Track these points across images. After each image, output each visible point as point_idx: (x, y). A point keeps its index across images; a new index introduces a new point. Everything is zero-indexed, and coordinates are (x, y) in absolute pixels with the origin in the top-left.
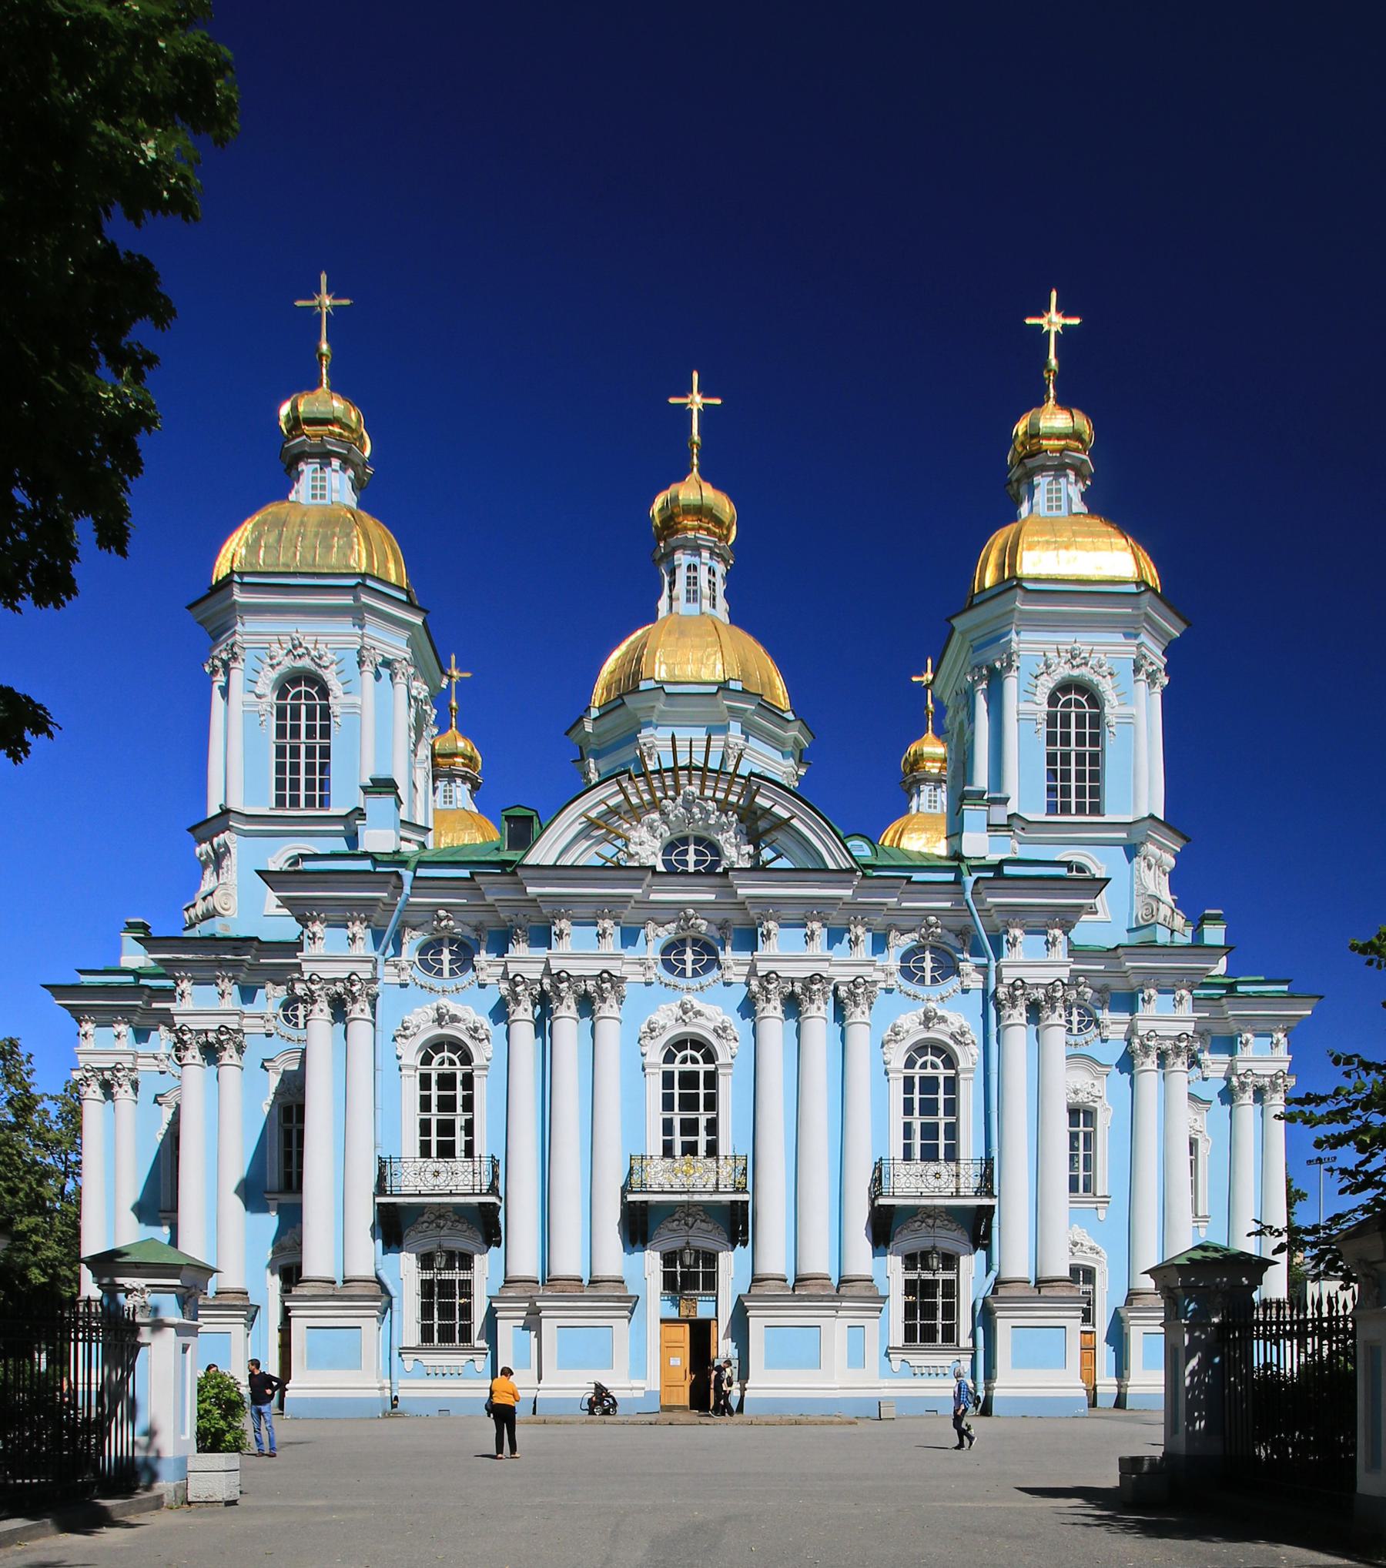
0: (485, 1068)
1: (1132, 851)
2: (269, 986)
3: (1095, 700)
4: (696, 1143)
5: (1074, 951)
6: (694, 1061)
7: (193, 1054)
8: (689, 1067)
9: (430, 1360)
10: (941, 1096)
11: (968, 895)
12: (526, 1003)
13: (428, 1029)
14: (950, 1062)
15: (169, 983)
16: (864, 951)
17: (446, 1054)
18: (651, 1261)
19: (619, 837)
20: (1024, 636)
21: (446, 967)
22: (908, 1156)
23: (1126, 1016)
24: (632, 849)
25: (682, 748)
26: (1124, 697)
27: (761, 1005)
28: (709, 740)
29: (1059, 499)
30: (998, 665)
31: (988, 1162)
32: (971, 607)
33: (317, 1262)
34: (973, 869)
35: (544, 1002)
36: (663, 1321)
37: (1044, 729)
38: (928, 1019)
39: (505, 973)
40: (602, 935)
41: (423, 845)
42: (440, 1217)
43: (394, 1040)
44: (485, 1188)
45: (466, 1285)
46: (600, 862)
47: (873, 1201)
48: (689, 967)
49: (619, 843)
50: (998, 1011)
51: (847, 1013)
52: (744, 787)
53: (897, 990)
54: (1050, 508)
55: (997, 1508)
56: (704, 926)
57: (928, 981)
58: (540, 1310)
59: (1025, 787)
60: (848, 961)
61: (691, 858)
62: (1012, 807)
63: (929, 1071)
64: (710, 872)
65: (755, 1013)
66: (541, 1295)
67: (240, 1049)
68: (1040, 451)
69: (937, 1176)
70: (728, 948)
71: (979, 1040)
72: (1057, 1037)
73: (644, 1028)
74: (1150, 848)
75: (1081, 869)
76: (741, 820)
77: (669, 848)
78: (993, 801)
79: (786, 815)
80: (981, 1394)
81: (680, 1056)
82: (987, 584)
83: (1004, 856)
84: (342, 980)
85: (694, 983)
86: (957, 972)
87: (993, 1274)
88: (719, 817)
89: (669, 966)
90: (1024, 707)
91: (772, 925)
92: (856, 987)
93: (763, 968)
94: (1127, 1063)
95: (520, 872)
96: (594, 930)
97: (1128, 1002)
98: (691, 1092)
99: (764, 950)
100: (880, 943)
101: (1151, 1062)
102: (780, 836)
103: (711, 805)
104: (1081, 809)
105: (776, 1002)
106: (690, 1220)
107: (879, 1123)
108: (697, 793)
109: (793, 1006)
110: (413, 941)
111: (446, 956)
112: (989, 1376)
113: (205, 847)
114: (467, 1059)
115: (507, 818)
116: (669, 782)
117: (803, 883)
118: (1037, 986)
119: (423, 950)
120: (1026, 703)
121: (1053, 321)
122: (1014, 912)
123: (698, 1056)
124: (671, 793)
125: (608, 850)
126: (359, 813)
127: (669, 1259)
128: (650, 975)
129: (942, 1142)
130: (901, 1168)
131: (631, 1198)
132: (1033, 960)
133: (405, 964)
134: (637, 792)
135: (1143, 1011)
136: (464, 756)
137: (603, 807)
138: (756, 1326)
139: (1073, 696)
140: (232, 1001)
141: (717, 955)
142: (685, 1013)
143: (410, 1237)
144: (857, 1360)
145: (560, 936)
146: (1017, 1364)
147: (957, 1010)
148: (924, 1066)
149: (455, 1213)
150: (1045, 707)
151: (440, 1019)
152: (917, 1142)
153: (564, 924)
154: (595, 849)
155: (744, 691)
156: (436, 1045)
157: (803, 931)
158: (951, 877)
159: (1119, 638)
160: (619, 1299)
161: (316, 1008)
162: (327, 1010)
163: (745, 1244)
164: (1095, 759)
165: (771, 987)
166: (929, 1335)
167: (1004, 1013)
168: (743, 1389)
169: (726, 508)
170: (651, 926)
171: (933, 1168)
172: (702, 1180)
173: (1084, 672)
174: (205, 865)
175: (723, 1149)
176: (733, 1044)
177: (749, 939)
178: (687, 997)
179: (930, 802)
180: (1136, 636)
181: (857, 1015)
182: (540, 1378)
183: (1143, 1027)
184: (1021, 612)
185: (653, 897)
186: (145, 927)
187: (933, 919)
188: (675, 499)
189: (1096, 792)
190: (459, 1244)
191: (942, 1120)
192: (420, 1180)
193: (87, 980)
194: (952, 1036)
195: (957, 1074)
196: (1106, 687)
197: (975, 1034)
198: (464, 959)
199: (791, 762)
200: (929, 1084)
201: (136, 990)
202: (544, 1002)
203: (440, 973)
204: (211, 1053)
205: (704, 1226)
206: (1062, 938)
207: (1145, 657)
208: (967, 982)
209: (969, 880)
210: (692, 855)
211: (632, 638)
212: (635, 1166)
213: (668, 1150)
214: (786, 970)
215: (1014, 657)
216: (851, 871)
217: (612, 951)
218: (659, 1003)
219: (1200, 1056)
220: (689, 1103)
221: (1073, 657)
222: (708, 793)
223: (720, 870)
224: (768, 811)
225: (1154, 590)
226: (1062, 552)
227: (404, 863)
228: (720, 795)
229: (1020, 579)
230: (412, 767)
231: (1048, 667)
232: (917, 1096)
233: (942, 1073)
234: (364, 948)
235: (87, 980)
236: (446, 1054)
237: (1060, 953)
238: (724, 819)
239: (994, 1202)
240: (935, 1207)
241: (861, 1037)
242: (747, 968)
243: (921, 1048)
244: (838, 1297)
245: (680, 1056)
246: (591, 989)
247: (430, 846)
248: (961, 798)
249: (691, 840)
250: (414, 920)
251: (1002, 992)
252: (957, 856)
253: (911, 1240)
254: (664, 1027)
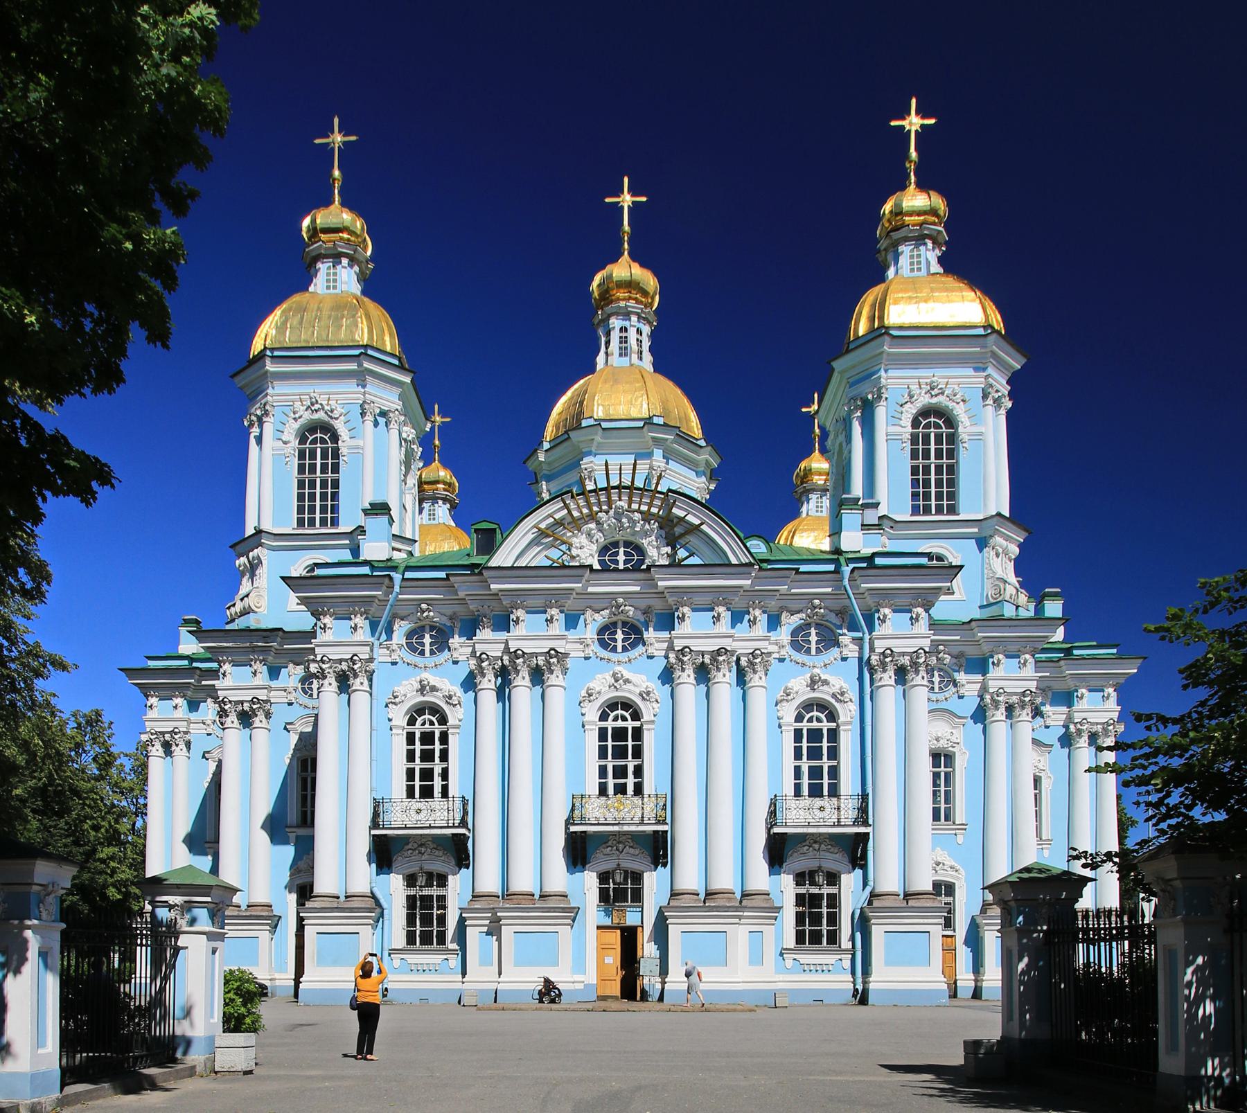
0: (458, 727)
1: (982, 543)
2: (291, 666)
3: (951, 422)
4: (625, 784)
5: (934, 625)
6: (624, 719)
7: (232, 720)
8: (620, 723)
9: (413, 959)
10: (825, 744)
11: (846, 582)
12: (490, 675)
13: (413, 697)
14: (832, 717)
15: (215, 665)
16: (761, 629)
17: (427, 717)
18: (590, 880)
19: (564, 543)
20: (891, 373)
21: (427, 648)
22: (798, 793)
23: (979, 677)
24: (574, 552)
25: (614, 471)
26: (975, 418)
27: (677, 673)
28: (635, 464)
29: (919, 263)
30: (870, 397)
31: (864, 797)
32: (848, 351)
33: (326, 881)
34: (849, 560)
35: (505, 675)
36: (599, 928)
37: (908, 446)
38: (813, 683)
39: (474, 652)
40: (549, 621)
41: (410, 554)
42: (421, 845)
43: (387, 706)
44: (457, 822)
45: (442, 899)
46: (549, 563)
47: (769, 830)
48: (620, 645)
49: (564, 547)
50: (871, 675)
51: (747, 679)
52: (663, 501)
53: (788, 660)
54: (912, 270)
55: (860, 1081)
56: (631, 611)
57: (813, 651)
58: (500, 919)
59: (893, 495)
60: (747, 638)
61: (621, 558)
62: (882, 510)
63: (815, 724)
64: (636, 569)
65: (672, 680)
66: (501, 907)
67: (268, 715)
68: (904, 226)
69: (822, 809)
70: (651, 629)
71: (856, 698)
72: (920, 695)
73: (584, 693)
74: (998, 540)
75: (940, 558)
76: (661, 527)
77: (603, 550)
78: (866, 506)
79: (697, 522)
80: (860, 987)
81: (612, 715)
82: (861, 333)
83: (875, 550)
84: (346, 660)
85: (624, 657)
86: (837, 644)
87: (868, 889)
88: (643, 526)
89: (603, 644)
90: (892, 429)
91: (686, 610)
92: (755, 658)
93: (678, 644)
94: (980, 715)
95: (485, 573)
96: (544, 616)
97: (980, 665)
98: (621, 743)
99: (679, 629)
100: (774, 622)
101: (1000, 714)
102: (692, 540)
103: (637, 516)
104: (939, 510)
105: (690, 671)
106: (621, 846)
107: (775, 766)
108: (626, 507)
109: (703, 674)
110: (401, 629)
111: (427, 640)
112: (866, 972)
113: (243, 560)
114: (443, 720)
115: (476, 530)
116: (603, 499)
117: (712, 576)
118: (904, 654)
119: (409, 635)
120: (893, 427)
121: (914, 122)
122: (885, 594)
123: (627, 715)
124: (605, 507)
125: (555, 554)
126: (361, 530)
127: (604, 877)
128: (589, 651)
129: (826, 781)
130: (792, 803)
131: (573, 829)
132: (899, 633)
133: (395, 647)
134: (578, 508)
135: (993, 672)
136: (444, 483)
137: (551, 520)
138: (674, 932)
139: (932, 420)
140: (262, 678)
141: (642, 634)
142: (616, 681)
143: (398, 861)
144: (756, 958)
145: (517, 622)
146: (888, 963)
147: (837, 674)
148: (810, 720)
149: (433, 842)
150: (910, 430)
151: (422, 690)
152: (805, 781)
153: (520, 613)
154: (545, 553)
155: (665, 425)
156: (420, 710)
157: (711, 614)
158: (831, 567)
159: (970, 372)
160: (564, 910)
161: (326, 682)
162: (335, 684)
163: (665, 865)
164: (951, 469)
165: (685, 659)
166: (816, 938)
167: (877, 676)
168: (663, 983)
169: (650, 281)
170: (589, 612)
171: (818, 802)
172: (630, 814)
173: (941, 399)
174: (243, 574)
175: (648, 789)
176: (655, 705)
177: (667, 621)
178: (618, 668)
179: (816, 507)
180: (984, 369)
181: (756, 680)
182: (500, 974)
183: (993, 686)
184: (889, 354)
185: (590, 589)
186: (198, 622)
187: (817, 602)
189: (952, 496)
190: (437, 867)
191: (826, 764)
192: (406, 816)
193: (153, 664)
194: (834, 696)
195: (838, 726)
196: (959, 411)
197: (853, 694)
198: (441, 643)
199: (703, 479)
200: (815, 735)
201: (190, 671)
202: (505, 675)
203: (422, 653)
204: (246, 719)
205: (632, 851)
206: (924, 615)
207: (991, 386)
208: (845, 652)
209: (846, 570)
210: (623, 556)
211: (576, 386)
212: (576, 803)
213: (603, 791)
214: (697, 645)
215: (883, 390)
216: (750, 565)
217: (558, 633)
218: (594, 674)
219: (1043, 708)
220: (620, 753)
221: (932, 389)
222: (634, 506)
223: (644, 567)
224: (682, 519)
225: (998, 332)
226: (922, 305)
227: (394, 568)
228: (644, 508)
229: (888, 328)
230: (402, 493)
231: (911, 397)
232: (805, 744)
233: (826, 725)
234: (363, 635)
235: (153, 664)
236: (427, 717)
237: (922, 627)
238: (647, 526)
239: (869, 830)
240: (820, 834)
241: (759, 697)
242: (666, 645)
243: (808, 706)
244: (740, 907)
245: (612, 715)
246: (541, 663)
247: (417, 554)
248: (841, 504)
249: (621, 544)
250: (402, 612)
251: (875, 659)
252: (837, 551)
253: (800, 861)
254: (599, 693)
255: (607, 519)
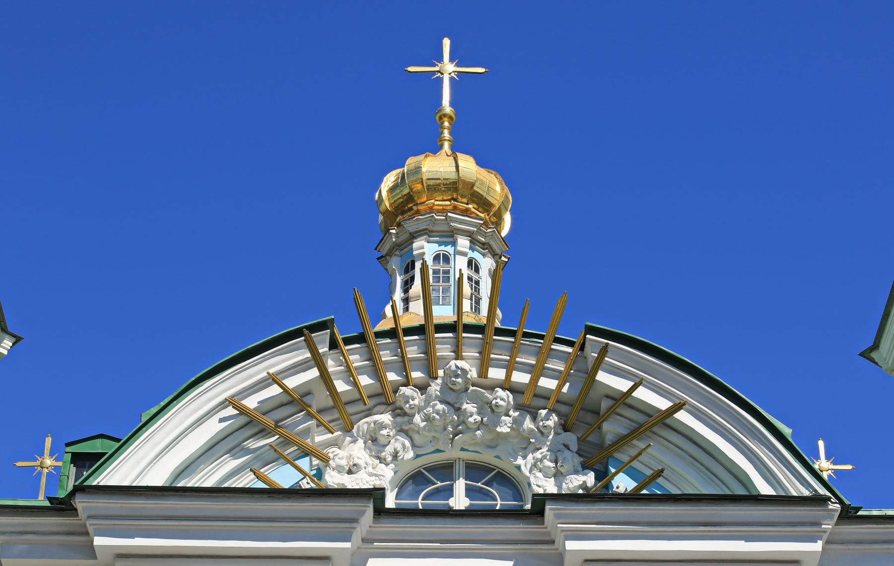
19: (306, 453)
52: (571, 361)
76: (565, 427)
88: (517, 422)
108: (473, 374)
116: (413, 352)
188: (418, 170)
216: (817, 500)
222: (496, 374)
238: (528, 424)
249: (460, 468)
255: (424, 404)
